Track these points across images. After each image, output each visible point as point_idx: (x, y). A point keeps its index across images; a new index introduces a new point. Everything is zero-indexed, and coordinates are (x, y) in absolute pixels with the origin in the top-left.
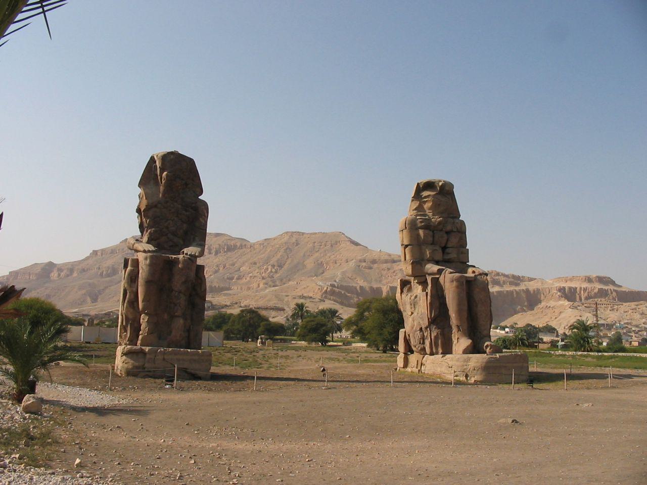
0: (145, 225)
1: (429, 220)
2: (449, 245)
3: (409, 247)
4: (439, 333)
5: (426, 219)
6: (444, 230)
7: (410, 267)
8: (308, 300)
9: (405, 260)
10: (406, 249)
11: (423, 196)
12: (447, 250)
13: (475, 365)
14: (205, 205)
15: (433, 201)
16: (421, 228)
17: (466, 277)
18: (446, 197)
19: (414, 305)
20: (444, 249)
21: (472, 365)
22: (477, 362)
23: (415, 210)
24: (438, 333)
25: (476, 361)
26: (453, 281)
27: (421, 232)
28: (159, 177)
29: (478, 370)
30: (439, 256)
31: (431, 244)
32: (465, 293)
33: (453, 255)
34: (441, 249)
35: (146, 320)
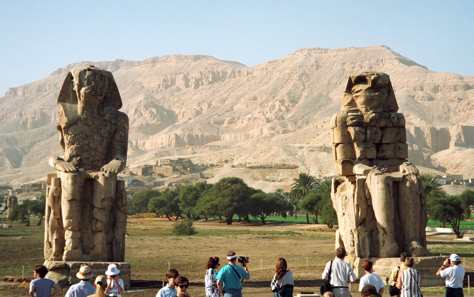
0: (66, 142)
1: (362, 116)
2: (385, 141)
3: (340, 145)
5: (357, 115)
7: (340, 167)
9: (336, 159)
10: (337, 148)
14: (125, 117)
16: (353, 125)
17: (393, 178)
19: (345, 206)
27: (351, 130)
28: (77, 94)
30: (372, 154)
32: (392, 194)
33: (388, 152)
34: (374, 145)
35: (70, 236)
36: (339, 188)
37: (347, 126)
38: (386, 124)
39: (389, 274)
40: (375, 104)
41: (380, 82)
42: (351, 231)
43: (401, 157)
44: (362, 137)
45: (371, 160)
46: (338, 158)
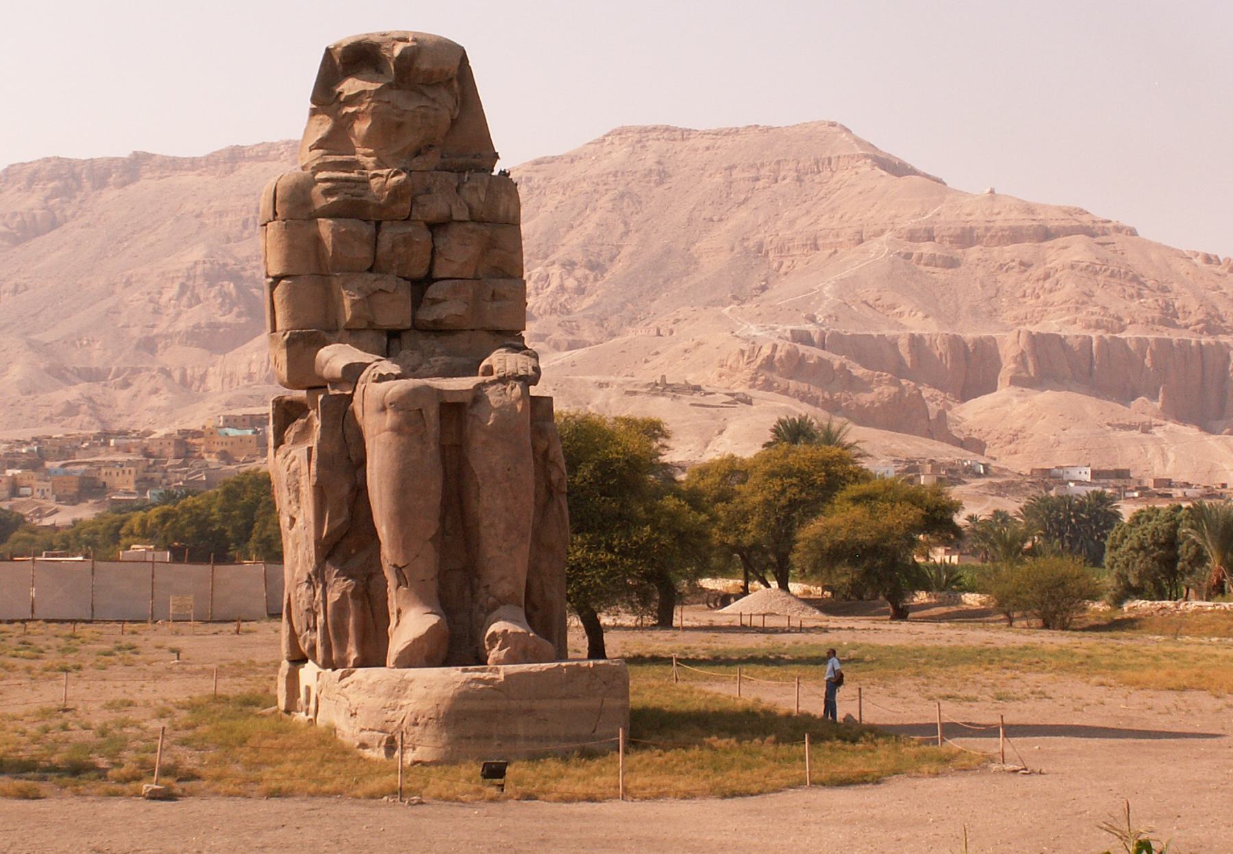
4: (349, 591)
5: (347, 180)
6: (416, 215)
8: (687, 399)
9: (274, 330)
11: (342, 98)
12: (433, 291)
13: (418, 706)
15: (373, 113)
18: (423, 94)
20: (420, 286)
21: (411, 708)
22: (425, 697)
23: (320, 145)
24: (344, 594)
25: (425, 691)
26: (384, 409)
27: (325, 227)
29: (426, 725)
31: (370, 270)
32: (433, 447)
33: (448, 306)
36: (290, 434)
37: (313, 217)
38: (445, 210)
39: (396, 724)
40: (411, 139)
41: (424, 65)
42: (309, 577)
43: (503, 325)
44: (362, 253)
45: (394, 335)
46: (279, 326)
